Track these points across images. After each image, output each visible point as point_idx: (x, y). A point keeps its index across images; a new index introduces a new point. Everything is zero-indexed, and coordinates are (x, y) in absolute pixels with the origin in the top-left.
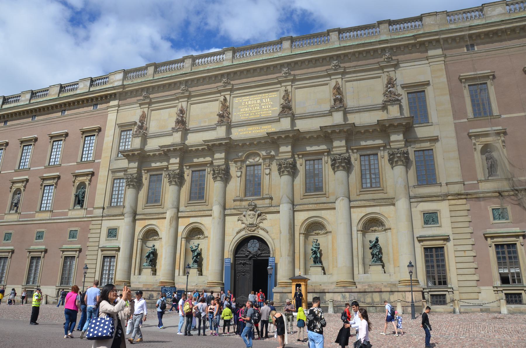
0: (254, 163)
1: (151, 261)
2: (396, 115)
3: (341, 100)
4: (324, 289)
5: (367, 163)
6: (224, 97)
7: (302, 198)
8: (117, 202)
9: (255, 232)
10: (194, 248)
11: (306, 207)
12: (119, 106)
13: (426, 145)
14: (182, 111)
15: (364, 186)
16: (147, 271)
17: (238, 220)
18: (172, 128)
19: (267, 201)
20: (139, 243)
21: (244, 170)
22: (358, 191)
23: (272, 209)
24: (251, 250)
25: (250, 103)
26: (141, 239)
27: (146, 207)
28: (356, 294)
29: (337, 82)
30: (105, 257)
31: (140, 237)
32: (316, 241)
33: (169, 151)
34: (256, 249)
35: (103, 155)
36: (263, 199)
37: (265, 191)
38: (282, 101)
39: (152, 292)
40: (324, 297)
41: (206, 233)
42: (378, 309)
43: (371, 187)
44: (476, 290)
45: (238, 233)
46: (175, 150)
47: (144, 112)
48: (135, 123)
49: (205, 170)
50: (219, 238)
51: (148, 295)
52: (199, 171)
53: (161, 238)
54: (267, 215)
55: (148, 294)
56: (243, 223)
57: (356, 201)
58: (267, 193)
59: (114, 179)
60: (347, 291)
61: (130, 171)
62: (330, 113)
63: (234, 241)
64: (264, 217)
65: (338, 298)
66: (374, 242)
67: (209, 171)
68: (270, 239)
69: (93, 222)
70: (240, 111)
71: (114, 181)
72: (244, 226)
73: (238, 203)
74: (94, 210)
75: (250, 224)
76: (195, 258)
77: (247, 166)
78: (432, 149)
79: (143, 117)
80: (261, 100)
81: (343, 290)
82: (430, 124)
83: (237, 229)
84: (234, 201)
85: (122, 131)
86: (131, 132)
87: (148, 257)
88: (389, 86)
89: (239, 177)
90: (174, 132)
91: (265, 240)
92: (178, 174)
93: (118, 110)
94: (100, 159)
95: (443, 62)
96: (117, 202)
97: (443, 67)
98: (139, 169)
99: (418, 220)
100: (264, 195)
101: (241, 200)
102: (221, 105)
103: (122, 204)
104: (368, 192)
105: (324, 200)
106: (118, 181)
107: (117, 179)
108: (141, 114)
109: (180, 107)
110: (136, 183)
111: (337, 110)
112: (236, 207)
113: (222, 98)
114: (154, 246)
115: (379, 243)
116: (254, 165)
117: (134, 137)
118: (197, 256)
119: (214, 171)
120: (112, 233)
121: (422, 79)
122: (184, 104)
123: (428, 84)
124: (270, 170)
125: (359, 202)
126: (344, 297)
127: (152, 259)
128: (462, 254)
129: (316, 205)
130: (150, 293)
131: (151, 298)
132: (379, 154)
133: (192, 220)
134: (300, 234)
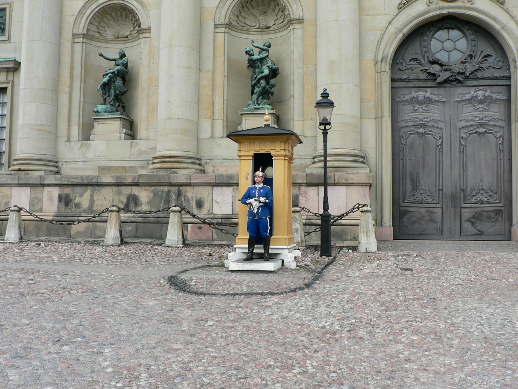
1: (117, 98)
16: (110, 129)
20: (78, 47)
26: (84, 36)
31: (81, 29)
39: (135, 191)
53: (148, 30)
55: (120, 193)
63: (392, 29)
87: (106, 87)
91: (497, 26)
118: (267, 78)
130: (127, 191)
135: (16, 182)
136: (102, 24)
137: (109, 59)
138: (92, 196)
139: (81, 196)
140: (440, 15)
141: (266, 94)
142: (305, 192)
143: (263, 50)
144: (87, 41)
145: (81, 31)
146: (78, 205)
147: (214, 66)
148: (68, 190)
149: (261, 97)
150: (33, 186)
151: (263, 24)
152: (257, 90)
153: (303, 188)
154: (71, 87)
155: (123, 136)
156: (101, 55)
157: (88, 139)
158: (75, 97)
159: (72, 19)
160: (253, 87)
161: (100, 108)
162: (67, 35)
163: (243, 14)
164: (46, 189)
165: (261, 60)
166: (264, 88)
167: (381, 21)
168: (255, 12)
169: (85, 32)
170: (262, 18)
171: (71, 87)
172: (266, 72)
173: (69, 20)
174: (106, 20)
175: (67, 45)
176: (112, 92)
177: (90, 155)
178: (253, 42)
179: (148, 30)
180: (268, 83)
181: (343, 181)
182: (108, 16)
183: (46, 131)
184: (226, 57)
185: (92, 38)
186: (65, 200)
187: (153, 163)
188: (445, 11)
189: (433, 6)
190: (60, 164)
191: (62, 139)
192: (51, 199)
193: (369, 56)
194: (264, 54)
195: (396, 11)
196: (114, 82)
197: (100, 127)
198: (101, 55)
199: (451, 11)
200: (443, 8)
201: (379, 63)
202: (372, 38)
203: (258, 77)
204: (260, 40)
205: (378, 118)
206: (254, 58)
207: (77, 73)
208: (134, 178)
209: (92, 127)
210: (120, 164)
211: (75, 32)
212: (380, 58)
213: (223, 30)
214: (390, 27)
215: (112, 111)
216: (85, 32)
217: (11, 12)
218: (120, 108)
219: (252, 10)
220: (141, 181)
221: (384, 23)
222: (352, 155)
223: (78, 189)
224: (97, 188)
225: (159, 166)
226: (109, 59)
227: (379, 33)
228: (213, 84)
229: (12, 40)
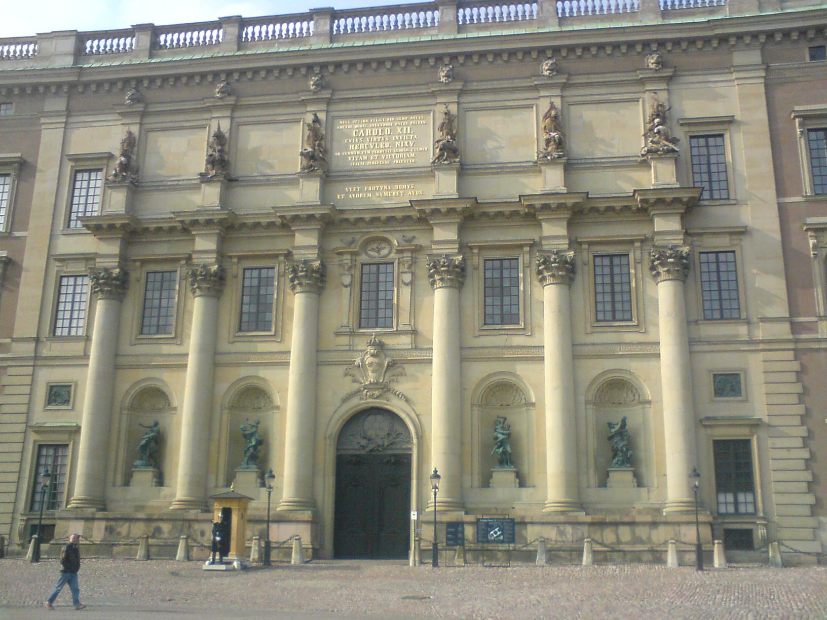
0: (377, 260)
1: (151, 456)
2: (667, 181)
3: (560, 144)
4: (523, 518)
5: (607, 271)
6: (315, 115)
7: (477, 333)
12: (69, 113)
13: (723, 242)
14: (219, 137)
15: (601, 316)
17: (346, 375)
18: (201, 174)
20: (125, 417)
22: (589, 325)
23: (415, 355)
24: (371, 433)
25: (368, 132)
29: (552, 103)
30: (41, 447)
32: (502, 420)
33: (195, 223)
35: (32, 224)
36: (398, 333)
38: (439, 135)
40: (524, 532)
42: (629, 557)
43: (614, 320)
44: (811, 522)
45: (345, 400)
46: (209, 222)
47: (130, 133)
48: (110, 157)
52: (260, 269)
54: (405, 366)
56: (355, 381)
59: (62, 277)
61: (101, 263)
62: (535, 168)
65: (551, 533)
66: (617, 427)
67: (282, 269)
69: (11, 371)
70: (347, 149)
71: (61, 282)
72: (356, 386)
74: (14, 345)
76: (251, 450)
77: (363, 265)
78: (734, 252)
79: (130, 145)
80: (393, 128)
81: (562, 518)
82: (733, 202)
84: (338, 334)
85: (77, 172)
86: (100, 175)
87: (144, 447)
88: (657, 120)
89: (346, 286)
90: (202, 182)
92: (216, 274)
93: (66, 123)
94: (26, 230)
95: (762, 81)
97: (762, 89)
98: (124, 259)
99: (707, 386)
101: (352, 334)
102: (307, 133)
108: (124, 136)
109: (214, 129)
110: (114, 286)
111: (553, 162)
113: (310, 118)
114: (156, 424)
115: (627, 428)
116: (378, 264)
117: (110, 188)
118: (255, 447)
119: (295, 271)
120: (59, 395)
121: (718, 110)
122: (225, 125)
123: (730, 121)
124: (413, 274)
125: (591, 348)
126: (562, 533)
127: (153, 451)
128: (784, 454)
130: (155, 524)
131: (157, 535)
132: (631, 256)
134: (472, 405)
135: (74, 516)
138: (129, 527)
141: (254, 458)
146: (119, 534)
148: (113, 523)
150: (87, 519)
152: (248, 454)
155: (154, 484)
161: (138, 462)
164: (96, 523)
186: (110, 530)
194: (254, 430)
218: (153, 463)
223: (120, 523)
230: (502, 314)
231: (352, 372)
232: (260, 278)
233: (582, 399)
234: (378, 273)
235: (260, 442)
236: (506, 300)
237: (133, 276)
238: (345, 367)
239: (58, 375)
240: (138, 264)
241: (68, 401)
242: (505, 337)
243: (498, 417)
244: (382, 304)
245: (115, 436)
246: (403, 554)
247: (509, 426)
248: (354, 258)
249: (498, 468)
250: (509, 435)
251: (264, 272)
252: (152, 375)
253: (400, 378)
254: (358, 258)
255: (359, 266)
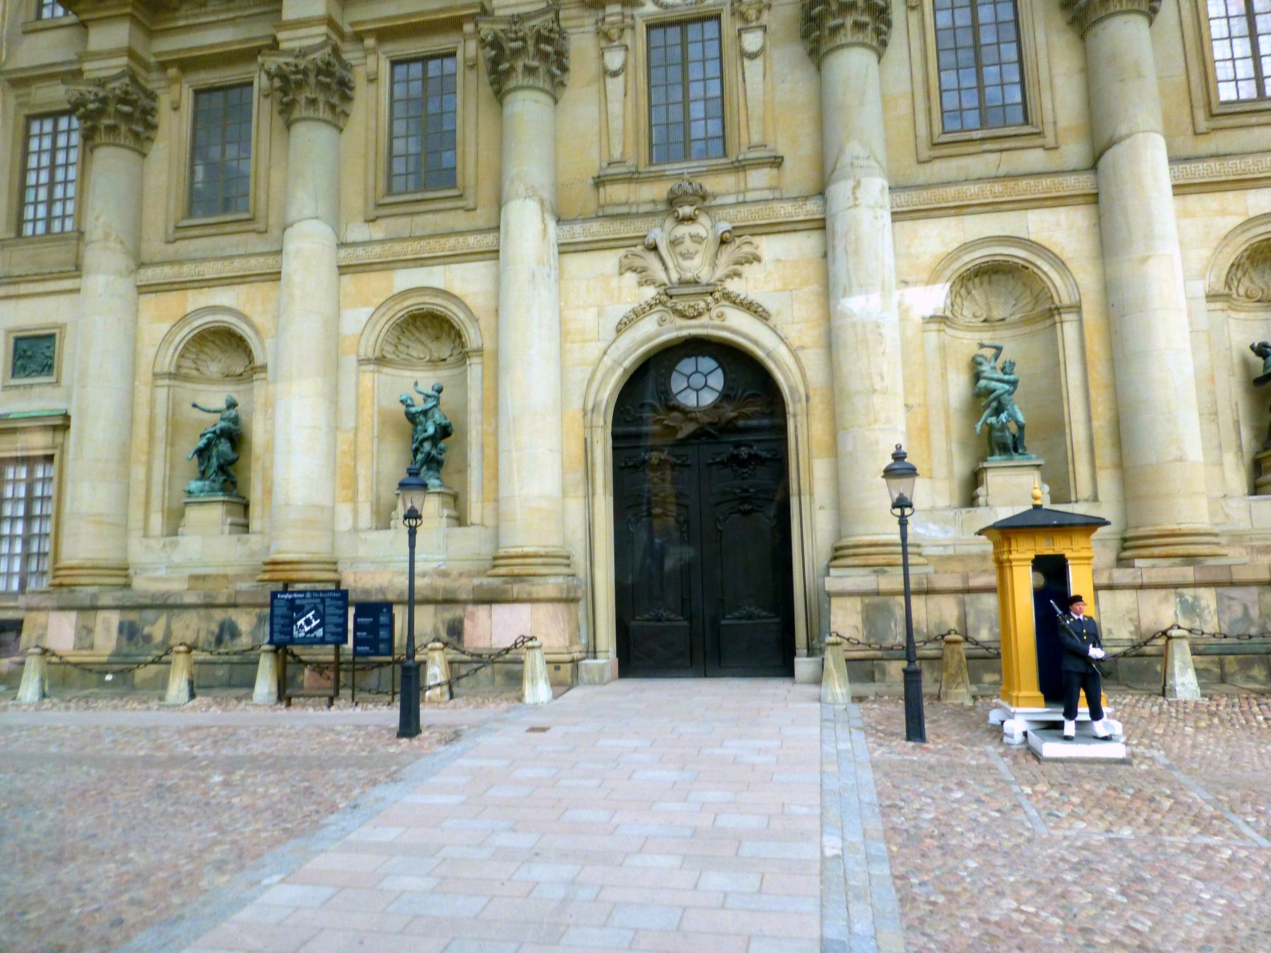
1: (222, 469)
7: (925, 153)
8: (49, 219)
9: (704, 320)
10: (419, 405)
11: (950, 195)
16: (210, 516)
17: (623, 269)
19: (759, 178)
20: (162, 393)
21: (638, 41)
22: (1201, 115)
26: (170, 376)
27: (179, 233)
28: (1254, 590)
32: (989, 353)
34: (708, 398)
36: (740, 167)
37: (751, 132)
39: (233, 614)
41: (473, 337)
45: (622, 327)
49: (452, 55)
50: (558, 339)
51: (215, 628)
52: (424, 59)
53: (264, 368)
55: (209, 619)
57: (1198, 158)
58: (756, 139)
59: (30, 118)
60: (1209, 578)
63: (607, 361)
64: (746, 249)
68: (782, 352)
72: (650, 292)
73: (617, 192)
75: (683, 283)
77: (650, 27)
83: (620, 310)
84: (599, 182)
87: (202, 453)
89: (615, 74)
91: (760, 353)
96: (49, 219)
100: (744, 149)
101: (633, 178)
103: (69, 225)
104: (1253, 119)
105: (1033, 159)
106: (48, 126)
107: (42, 117)
112: (609, 211)
116: (683, 23)
118: (434, 439)
125: (1214, 165)
126: (1190, 609)
127: (224, 460)
129: (998, 187)
130: (219, 615)
131: (227, 637)
133: (405, 279)
136: (203, 356)
137: (209, 411)
139: (153, 623)
140: (678, 338)
142: (473, 613)
143: (428, 396)
144: (176, 383)
145: (166, 369)
146: (148, 639)
147: (357, 422)
148: (132, 616)
149: (425, 468)
150: (81, 609)
151: (436, 355)
152: (420, 457)
153: (470, 608)
154: (150, 453)
155: (227, 528)
156: (195, 406)
157: (176, 534)
158: (166, 467)
159: (151, 352)
160: (416, 451)
161: (195, 485)
162: (145, 373)
163: (404, 340)
164: (102, 615)
165: (425, 413)
166: (429, 454)
167: (594, 350)
168: (423, 338)
169: (173, 370)
170: (433, 346)
171: (150, 453)
172: (431, 430)
173: (148, 352)
174: (206, 349)
175: (143, 392)
176: (214, 461)
177: (177, 558)
178: (416, 384)
179: (264, 368)
180: (435, 445)
181: (524, 596)
182: (211, 345)
183: (110, 524)
184: (376, 409)
185: (186, 378)
186: (129, 632)
187: (265, 571)
188: (685, 333)
189: (666, 326)
190: (131, 572)
191: (135, 535)
192: (107, 630)
193: (576, 404)
195: (613, 335)
196: (216, 445)
197: (193, 514)
198: (195, 406)
199: (694, 332)
200: (681, 328)
201: (589, 414)
202: (579, 376)
203: (420, 438)
204: (427, 379)
205: (589, 495)
206: (413, 410)
207: (160, 432)
208: (229, 596)
209: (182, 515)
210: (221, 571)
211: (158, 370)
212: (590, 406)
213: (372, 367)
214: (605, 358)
215: (213, 490)
216: (173, 370)
217: (62, 340)
219: (418, 335)
220: (240, 600)
221: (596, 353)
222: (541, 556)
223: (149, 614)
224: (176, 611)
225: (267, 576)
226: (209, 411)
227: (590, 369)
228: (355, 451)
229: (64, 381)
230: (982, 108)
231: (638, 263)
232: (425, 79)
233: (1200, 288)
234: (684, 44)
235: (444, 431)
236: (991, 73)
237: (164, 103)
238: (622, 252)
239: (31, 314)
240: (172, 72)
241: (51, 367)
242: (996, 156)
243: (982, 346)
244: (697, 110)
245: (142, 430)
246: (786, 670)
247: (1013, 364)
248: (628, 11)
249: (997, 460)
250: (1014, 383)
251: (433, 66)
252: (212, 303)
253: (746, 270)
254: (638, 12)
255: (641, 28)
